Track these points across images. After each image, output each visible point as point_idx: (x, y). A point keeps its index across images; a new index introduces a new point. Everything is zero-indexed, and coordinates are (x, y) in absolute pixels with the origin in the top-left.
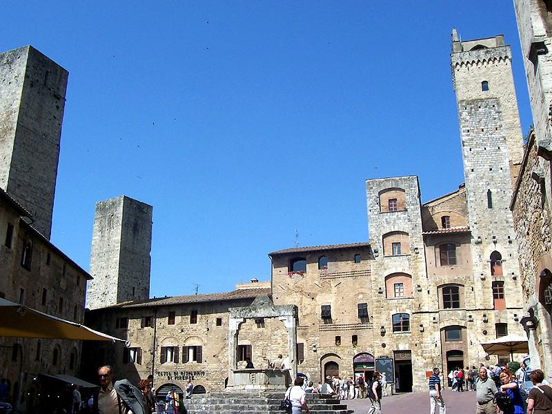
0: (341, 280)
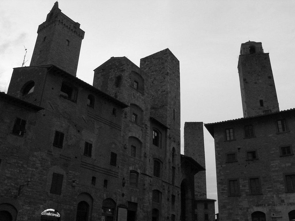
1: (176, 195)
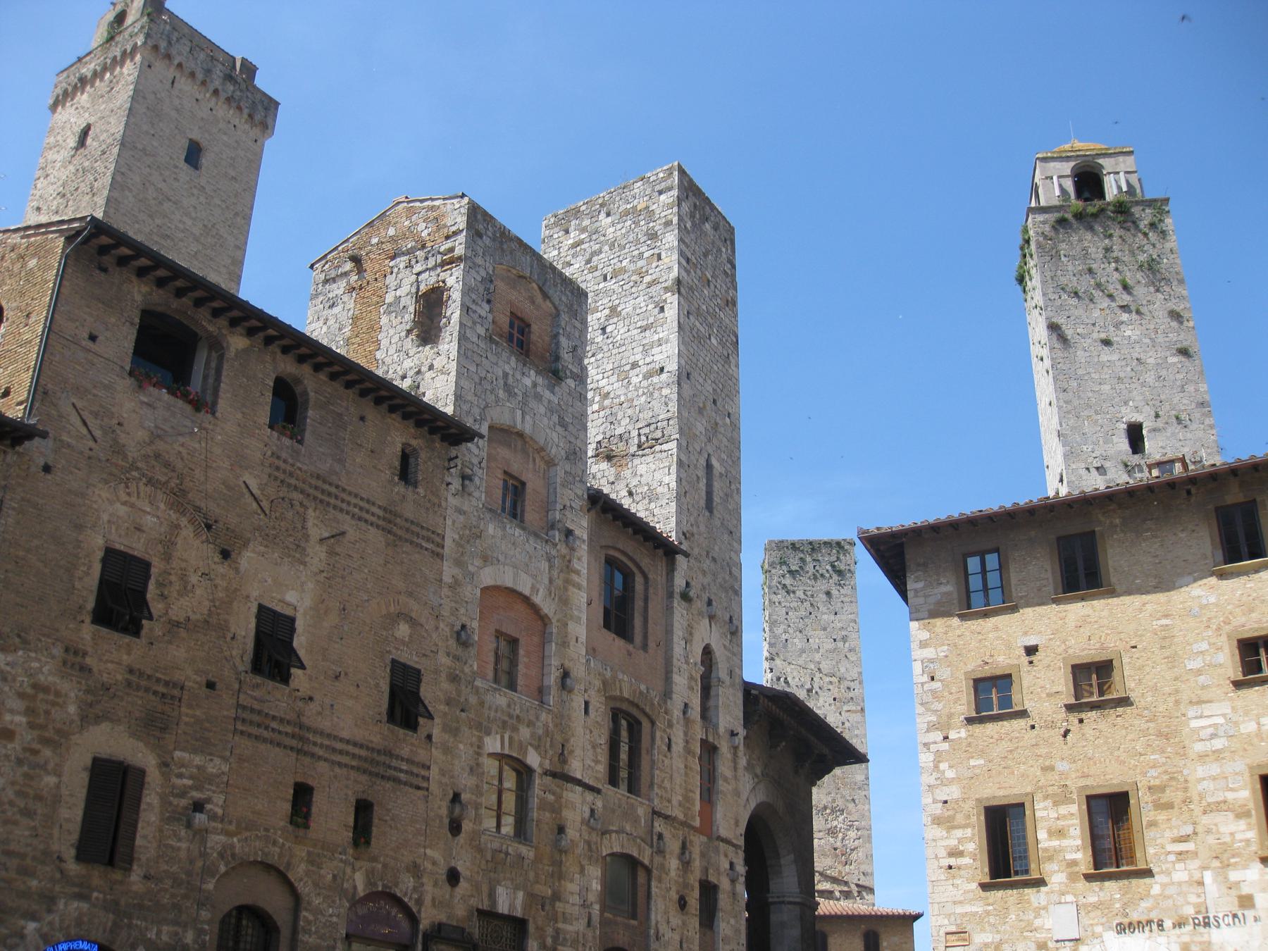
0: (348, 524)
1: (725, 884)
